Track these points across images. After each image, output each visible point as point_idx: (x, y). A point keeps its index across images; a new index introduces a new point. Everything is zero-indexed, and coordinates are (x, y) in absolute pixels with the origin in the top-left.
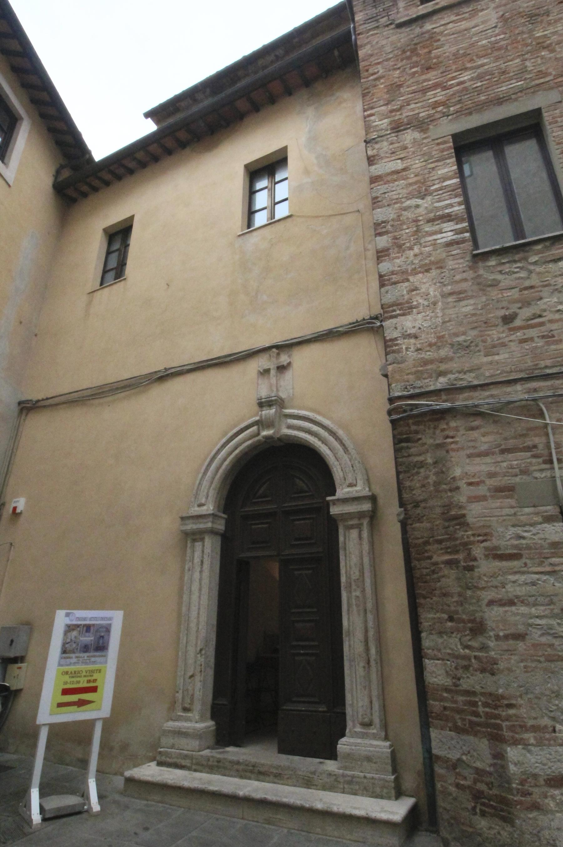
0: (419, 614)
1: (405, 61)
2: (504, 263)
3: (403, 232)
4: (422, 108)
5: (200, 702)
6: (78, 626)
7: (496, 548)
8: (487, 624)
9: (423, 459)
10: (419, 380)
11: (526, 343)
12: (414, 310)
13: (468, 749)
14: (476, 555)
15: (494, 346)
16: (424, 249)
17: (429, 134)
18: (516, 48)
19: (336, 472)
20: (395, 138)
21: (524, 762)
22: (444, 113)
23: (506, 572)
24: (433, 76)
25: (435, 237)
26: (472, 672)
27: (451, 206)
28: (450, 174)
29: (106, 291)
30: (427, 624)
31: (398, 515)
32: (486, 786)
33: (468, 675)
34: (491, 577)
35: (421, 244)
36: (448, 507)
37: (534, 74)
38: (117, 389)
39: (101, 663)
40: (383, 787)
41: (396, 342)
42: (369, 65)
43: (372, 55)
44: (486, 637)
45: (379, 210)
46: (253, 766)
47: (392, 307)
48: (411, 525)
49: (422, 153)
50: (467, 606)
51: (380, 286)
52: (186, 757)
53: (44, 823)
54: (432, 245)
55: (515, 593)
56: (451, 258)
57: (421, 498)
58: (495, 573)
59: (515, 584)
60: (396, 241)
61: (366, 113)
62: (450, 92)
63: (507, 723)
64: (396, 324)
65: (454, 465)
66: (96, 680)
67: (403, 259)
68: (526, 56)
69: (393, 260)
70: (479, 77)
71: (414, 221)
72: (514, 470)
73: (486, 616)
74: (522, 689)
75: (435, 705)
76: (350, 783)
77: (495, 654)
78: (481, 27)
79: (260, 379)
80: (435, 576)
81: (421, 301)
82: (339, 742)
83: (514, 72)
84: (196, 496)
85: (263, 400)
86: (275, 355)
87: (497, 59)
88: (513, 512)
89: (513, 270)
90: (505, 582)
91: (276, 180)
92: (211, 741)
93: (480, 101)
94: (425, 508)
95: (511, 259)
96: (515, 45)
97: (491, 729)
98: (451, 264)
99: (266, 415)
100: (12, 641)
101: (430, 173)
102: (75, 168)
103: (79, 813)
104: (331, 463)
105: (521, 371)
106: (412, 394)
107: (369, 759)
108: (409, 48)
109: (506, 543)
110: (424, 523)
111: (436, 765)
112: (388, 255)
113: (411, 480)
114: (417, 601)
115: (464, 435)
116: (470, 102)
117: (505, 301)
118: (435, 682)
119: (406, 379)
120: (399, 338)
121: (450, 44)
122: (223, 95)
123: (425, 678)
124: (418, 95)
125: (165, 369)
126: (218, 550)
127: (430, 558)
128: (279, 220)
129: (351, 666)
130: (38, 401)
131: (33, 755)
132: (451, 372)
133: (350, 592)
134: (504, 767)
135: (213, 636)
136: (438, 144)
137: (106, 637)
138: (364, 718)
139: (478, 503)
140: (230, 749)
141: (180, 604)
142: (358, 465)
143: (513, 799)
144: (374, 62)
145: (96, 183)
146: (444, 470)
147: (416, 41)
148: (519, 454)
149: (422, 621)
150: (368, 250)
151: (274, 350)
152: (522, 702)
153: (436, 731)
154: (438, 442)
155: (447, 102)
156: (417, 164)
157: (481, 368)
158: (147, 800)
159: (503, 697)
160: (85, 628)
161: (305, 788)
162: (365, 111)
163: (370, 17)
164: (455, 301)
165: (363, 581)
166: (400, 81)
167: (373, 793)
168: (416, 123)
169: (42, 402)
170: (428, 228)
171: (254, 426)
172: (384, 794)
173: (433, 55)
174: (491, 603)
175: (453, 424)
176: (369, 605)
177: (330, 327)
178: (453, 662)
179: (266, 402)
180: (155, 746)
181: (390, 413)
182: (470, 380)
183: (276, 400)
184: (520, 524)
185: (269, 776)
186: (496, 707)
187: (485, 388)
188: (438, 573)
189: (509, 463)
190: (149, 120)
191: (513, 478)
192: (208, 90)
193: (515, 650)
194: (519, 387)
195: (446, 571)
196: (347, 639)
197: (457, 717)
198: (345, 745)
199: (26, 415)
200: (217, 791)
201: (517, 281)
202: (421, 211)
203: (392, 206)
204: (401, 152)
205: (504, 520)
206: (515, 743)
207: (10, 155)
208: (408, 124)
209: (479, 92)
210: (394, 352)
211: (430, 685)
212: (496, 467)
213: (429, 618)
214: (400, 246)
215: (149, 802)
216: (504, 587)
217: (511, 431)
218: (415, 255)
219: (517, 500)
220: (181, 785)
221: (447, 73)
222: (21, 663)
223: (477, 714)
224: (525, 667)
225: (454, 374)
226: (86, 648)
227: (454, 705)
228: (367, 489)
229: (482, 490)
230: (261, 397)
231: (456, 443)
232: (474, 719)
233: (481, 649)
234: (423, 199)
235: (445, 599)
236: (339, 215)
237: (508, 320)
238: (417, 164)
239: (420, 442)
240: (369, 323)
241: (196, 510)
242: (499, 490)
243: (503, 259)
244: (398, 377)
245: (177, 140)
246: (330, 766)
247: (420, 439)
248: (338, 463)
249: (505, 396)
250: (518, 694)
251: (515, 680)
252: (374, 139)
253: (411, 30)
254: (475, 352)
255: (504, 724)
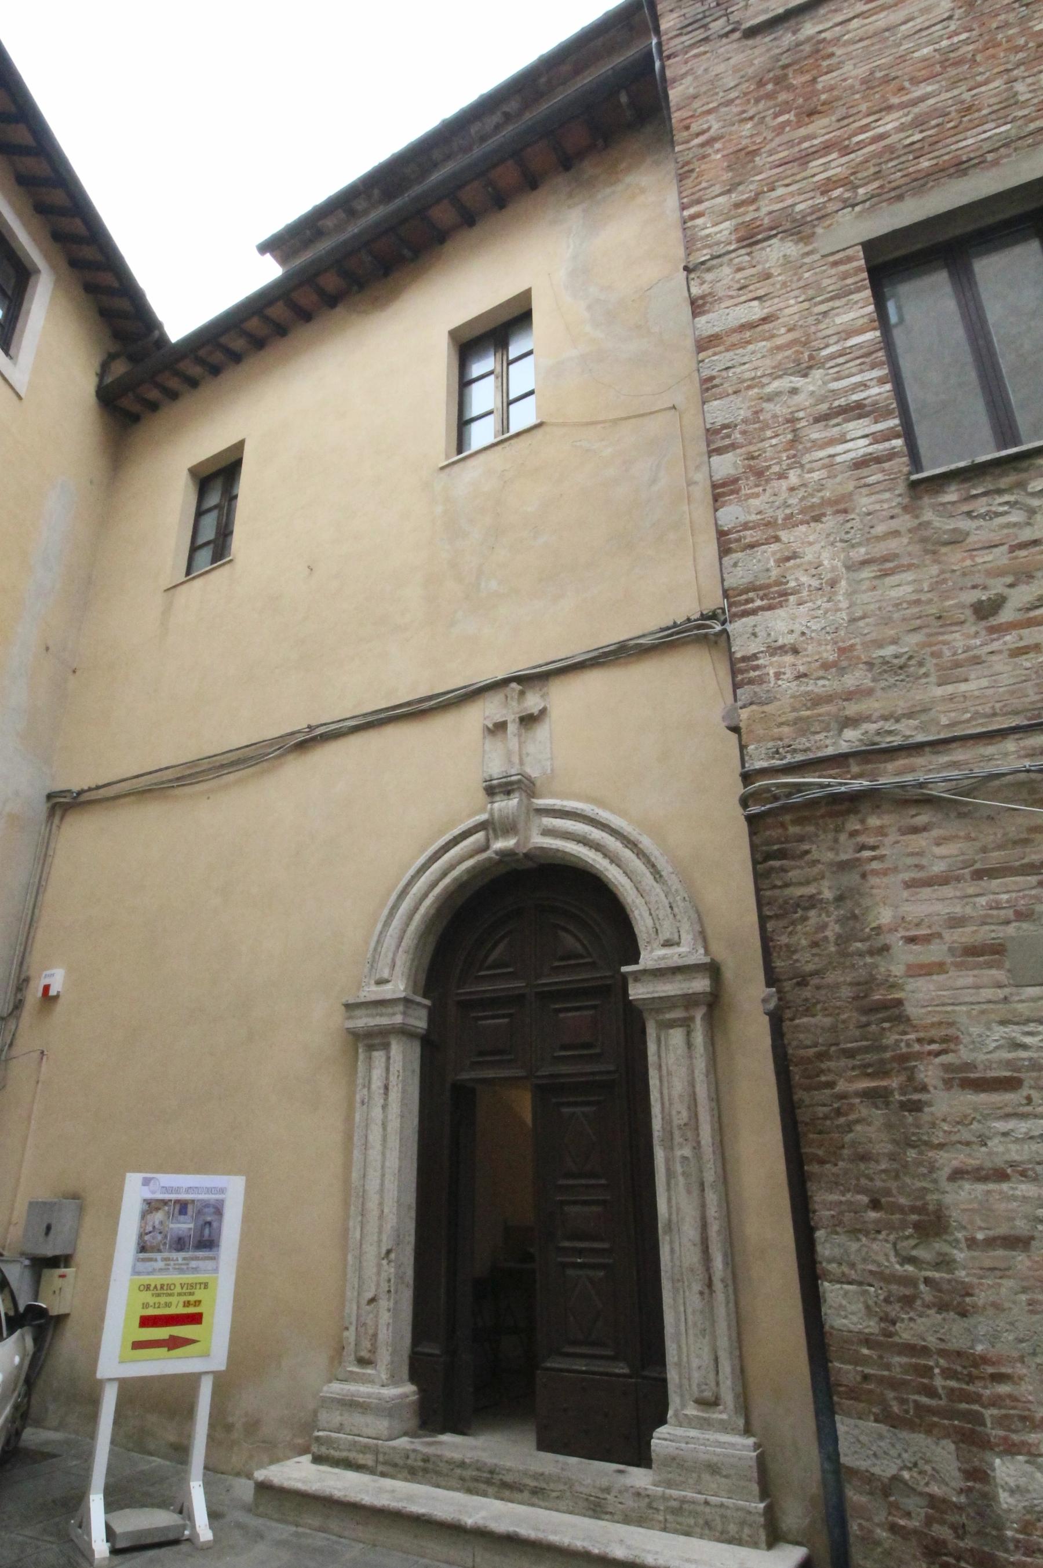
0: (809, 1194)
1: (763, 102)
2: (975, 496)
3: (766, 444)
4: (800, 194)
5: (390, 1348)
6: (165, 1202)
7: (970, 1066)
8: (950, 1217)
9: (814, 891)
10: (803, 735)
11: (1025, 657)
12: (791, 598)
13: (913, 1460)
14: (925, 1080)
15: (957, 665)
16: (809, 475)
17: (815, 245)
18: (993, 56)
19: (638, 917)
20: (747, 258)
21: (1030, 1488)
22: (845, 201)
23: (988, 1115)
24: (821, 129)
25: (831, 451)
26: (920, 1308)
27: (864, 385)
28: (861, 322)
29: (198, 583)
30: (828, 1213)
31: (765, 1001)
32: (950, 1531)
33: (912, 1314)
34: (958, 1123)
35: (802, 466)
36: (868, 983)
37: (1033, 108)
38: (222, 766)
39: (206, 1271)
40: (743, 1523)
41: (755, 663)
42: (692, 116)
43: (695, 97)
44: (950, 1243)
45: (716, 403)
46: (492, 1472)
47: (747, 593)
48: (792, 1019)
49: (801, 283)
50: (908, 1180)
51: (720, 552)
52: (365, 1449)
53: (114, 1557)
54: (824, 467)
55: (1007, 1157)
56: (864, 491)
57: (810, 968)
58: (966, 1116)
59: (1007, 1139)
60: (752, 463)
61: (686, 213)
62: (858, 156)
63: (995, 1411)
64: (755, 626)
65: (877, 904)
66: (200, 1301)
67: (765, 497)
68: (1015, 72)
69: (746, 500)
70: (919, 123)
71: (788, 421)
72: (1002, 912)
73: (948, 1199)
74: (1024, 1345)
75: (845, 1371)
76: (677, 1512)
77: (968, 1275)
78: (919, 20)
79: (487, 741)
80: (842, 1120)
81: (804, 579)
82: (655, 1434)
83: (989, 106)
84: (373, 963)
85: (495, 782)
86: (516, 695)
87: (954, 83)
88: (1002, 996)
89: (994, 509)
90: (987, 1133)
91: (511, 357)
92: (413, 1423)
93: (919, 171)
94: (818, 988)
95: (991, 487)
96: (991, 51)
97: (960, 1421)
98: (864, 502)
99: (500, 810)
100: (49, 1228)
101: (818, 322)
102: (134, 359)
103: (176, 1542)
104: (629, 900)
105: (1016, 713)
106: (790, 763)
107: (713, 1469)
108: (771, 75)
109: (989, 1056)
110: (819, 1017)
111: (848, 1486)
112: (737, 491)
113: (791, 933)
114: (806, 1168)
115: (897, 842)
116: (899, 174)
117: (979, 571)
118: (845, 1325)
119: (777, 736)
120: (761, 655)
121: (857, 61)
122: (398, 202)
123: (824, 1317)
124: (794, 168)
125: (309, 727)
126: (416, 1066)
127: (831, 1085)
128: (518, 435)
129: (675, 1290)
130: (80, 793)
131: (93, 1435)
132: (868, 719)
133: (672, 1149)
134: (989, 1498)
135: (411, 1226)
136: (835, 264)
137: (215, 1224)
138: (702, 1391)
139: (928, 978)
140: (446, 1438)
141: (348, 1166)
142: (681, 904)
143: (1006, 1560)
144: (699, 111)
145: (174, 383)
146: (857, 912)
147: (785, 60)
148: (1013, 879)
149: (817, 1207)
150: (696, 483)
151: (514, 685)
152: (1024, 1371)
153: (848, 1421)
154: (844, 857)
155: (852, 178)
156: (791, 308)
157: (930, 709)
158: (297, 1526)
159: (984, 1360)
160: (178, 1207)
161: (590, 1517)
162: (684, 207)
163: (691, 20)
164: (875, 577)
165: (697, 1128)
166: (754, 143)
167: (722, 1533)
168: (788, 226)
169: (88, 794)
170: (816, 433)
171: (477, 832)
172: (745, 1537)
173: (819, 86)
174: (957, 1175)
175: (874, 821)
176: (709, 1176)
177: (622, 639)
178: (881, 1288)
179: (500, 785)
180: (310, 1425)
181: (744, 802)
182: (908, 733)
183: (519, 781)
184: (1016, 1019)
185: (521, 1491)
186: (971, 1379)
187: (940, 748)
188: (846, 1115)
189: (992, 897)
190: (268, 256)
191: (1001, 928)
192: (376, 192)
193: (1008, 1269)
194: (1010, 745)
195: (864, 1110)
196: (667, 1238)
197: (890, 1395)
198: (665, 1439)
199: (62, 819)
200: (424, 1515)
201: (1006, 531)
202: (799, 399)
203: (743, 393)
204: (758, 285)
205: (983, 1012)
206: (1011, 1449)
207: (20, 342)
208: (772, 229)
209: (918, 154)
210: (751, 682)
211: (835, 1332)
212: (964, 906)
213: (831, 1203)
214: (759, 474)
215: (300, 1530)
216: (986, 1145)
217: (995, 834)
218: (792, 489)
219: (1009, 971)
220: (358, 1499)
221: (851, 120)
222: (66, 1267)
223: (931, 1392)
224: (1031, 1303)
225: (875, 722)
226: (180, 1244)
227: (886, 1373)
228: (702, 951)
229: (935, 952)
230: (491, 776)
231: (881, 858)
232: (924, 1400)
233: (937, 1264)
234: (805, 376)
235: (862, 1166)
236: (635, 417)
237: (985, 610)
238: (791, 308)
239: (808, 857)
240: (699, 627)
241: (372, 992)
242: (972, 951)
243: (974, 487)
244: (761, 732)
245: (321, 292)
246: (638, 1477)
247: (807, 852)
248: (643, 901)
249: (982, 764)
250: (1015, 1354)
251: (1008, 1327)
252: (703, 263)
253: (775, 39)
254: (920, 678)
255: (989, 1413)
